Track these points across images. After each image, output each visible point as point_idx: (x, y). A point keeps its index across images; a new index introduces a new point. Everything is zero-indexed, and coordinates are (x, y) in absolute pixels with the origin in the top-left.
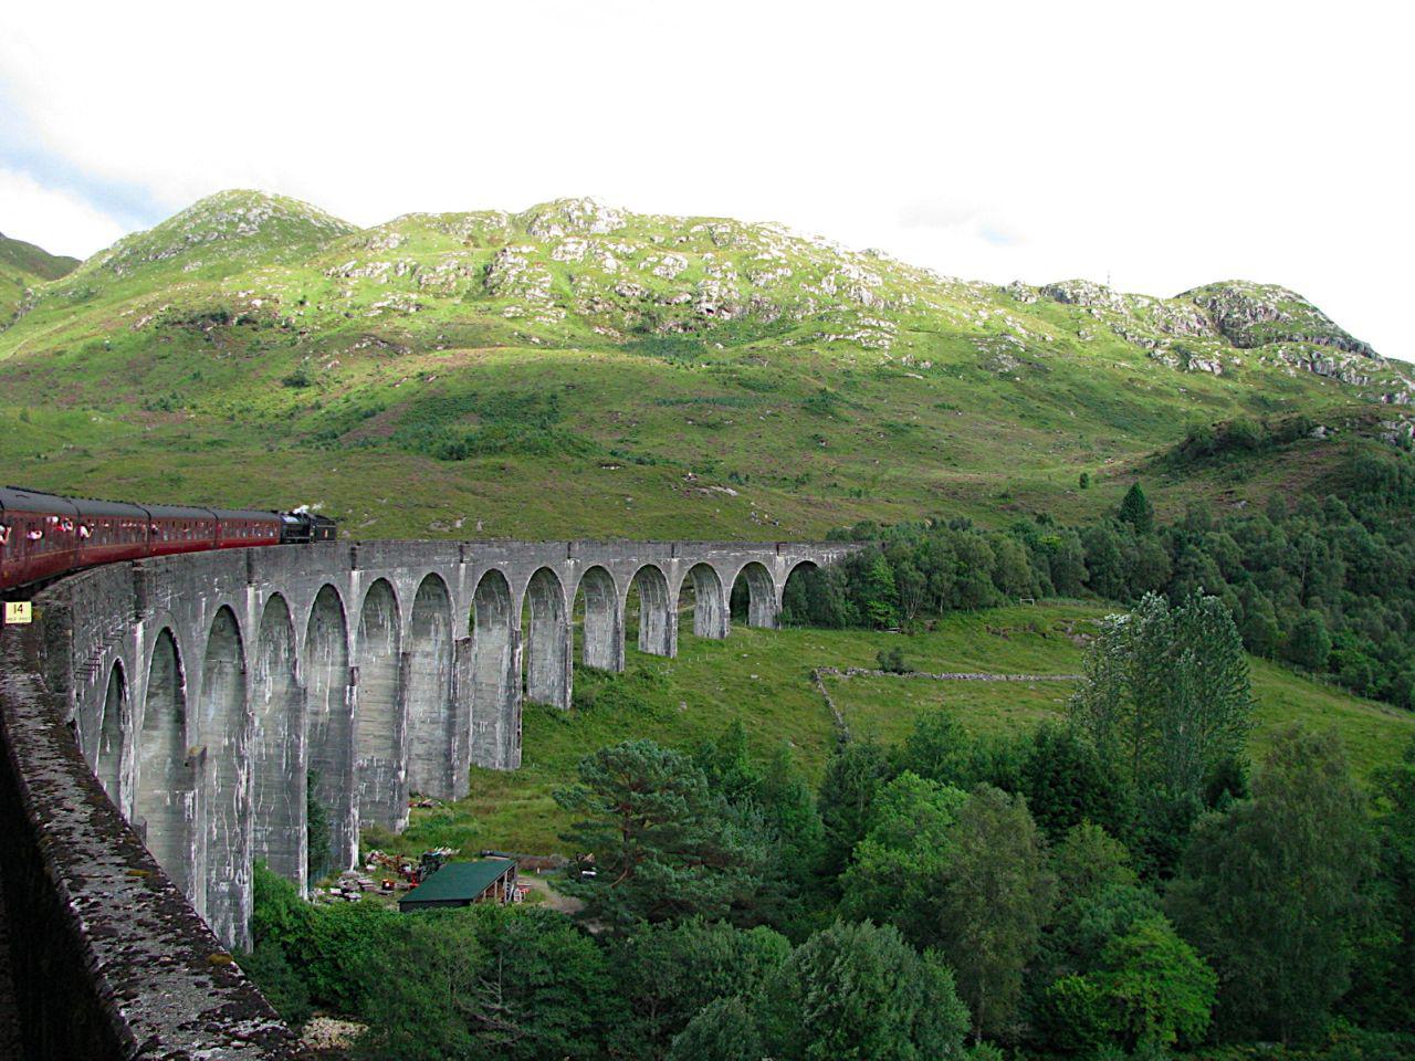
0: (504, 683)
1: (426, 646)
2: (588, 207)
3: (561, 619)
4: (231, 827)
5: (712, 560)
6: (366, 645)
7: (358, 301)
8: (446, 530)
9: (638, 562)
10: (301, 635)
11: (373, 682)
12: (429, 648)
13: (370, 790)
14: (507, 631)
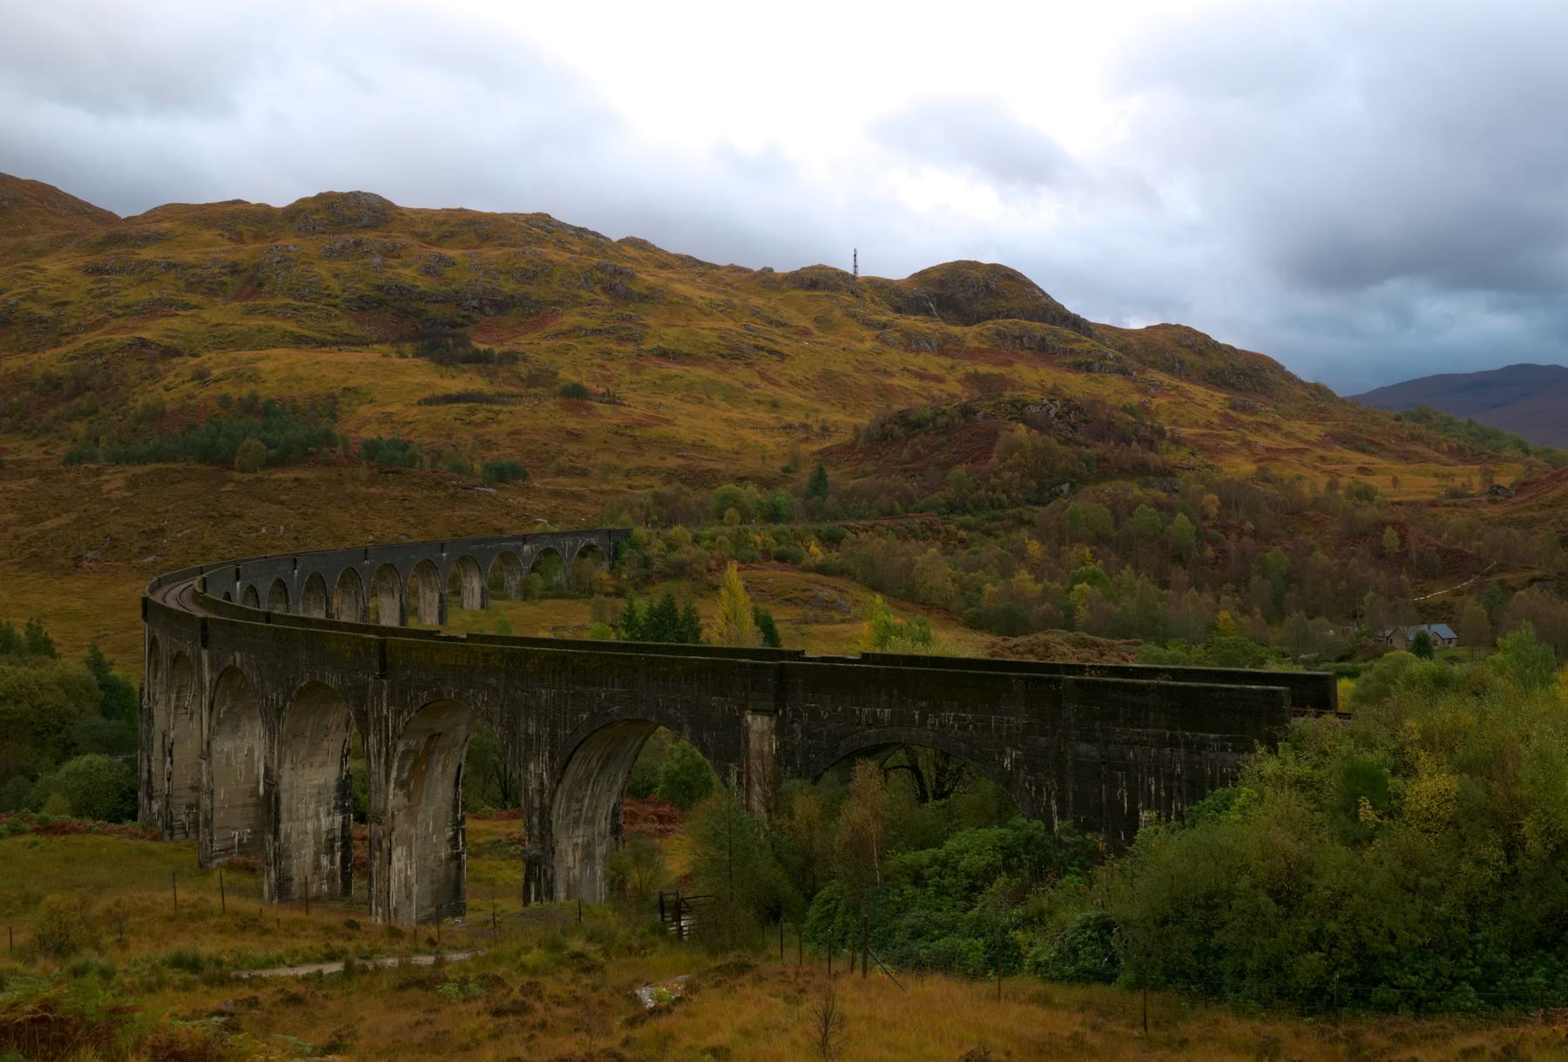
8: (254, 535)
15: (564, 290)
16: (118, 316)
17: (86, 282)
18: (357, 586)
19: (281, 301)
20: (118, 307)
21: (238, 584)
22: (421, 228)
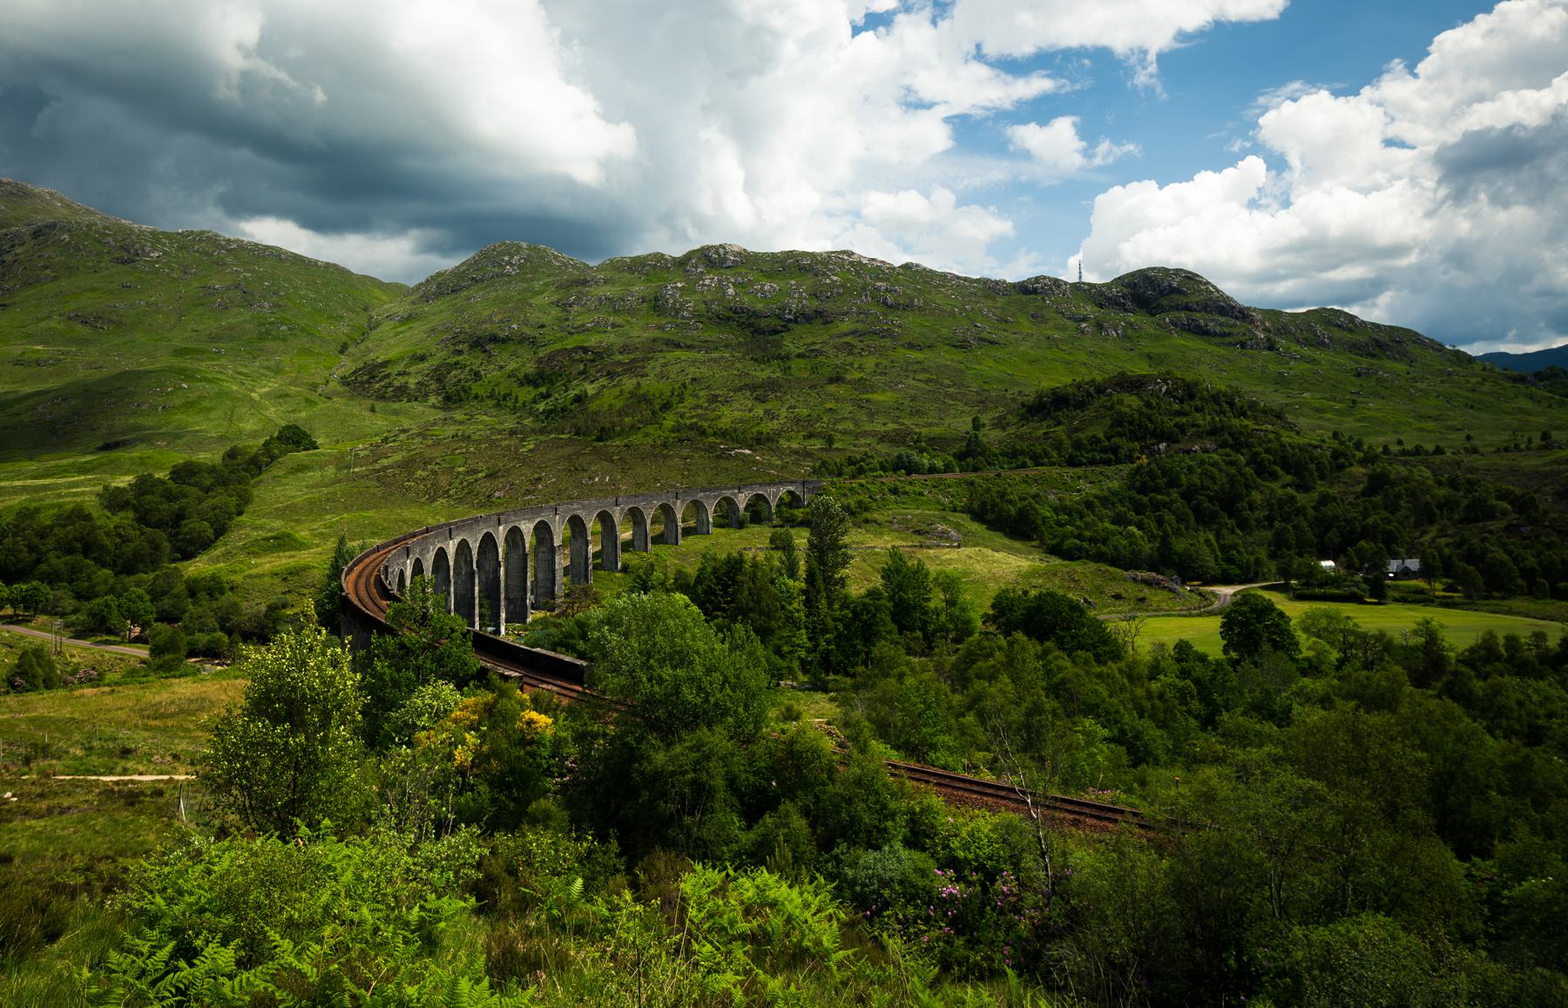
2: (721, 251)
7: (579, 323)
9: (657, 503)
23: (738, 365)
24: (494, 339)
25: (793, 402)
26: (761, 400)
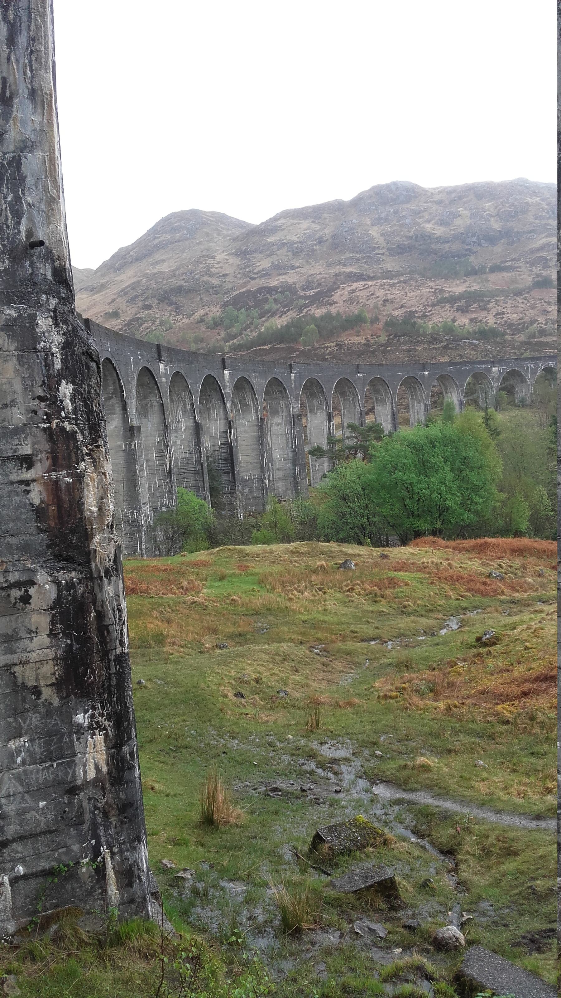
0: (326, 442)
1: (277, 420)
3: (358, 407)
4: (164, 480)
5: (450, 372)
6: (241, 416)
10: (197, 398)
11: (247, 435)
12: (280, 421)
13: (251, 491)
14: (325, 413)
15: (537, 221)
16: (255, 278)
17: (237, 261)
18: (353, 395)
19: (348, 255)
20: (254, 273)
21: (226, 372)
22: (437, 198)
23: (432, 284)
24: (179, 290)
25: (500, 309)
26: (464, 310)
